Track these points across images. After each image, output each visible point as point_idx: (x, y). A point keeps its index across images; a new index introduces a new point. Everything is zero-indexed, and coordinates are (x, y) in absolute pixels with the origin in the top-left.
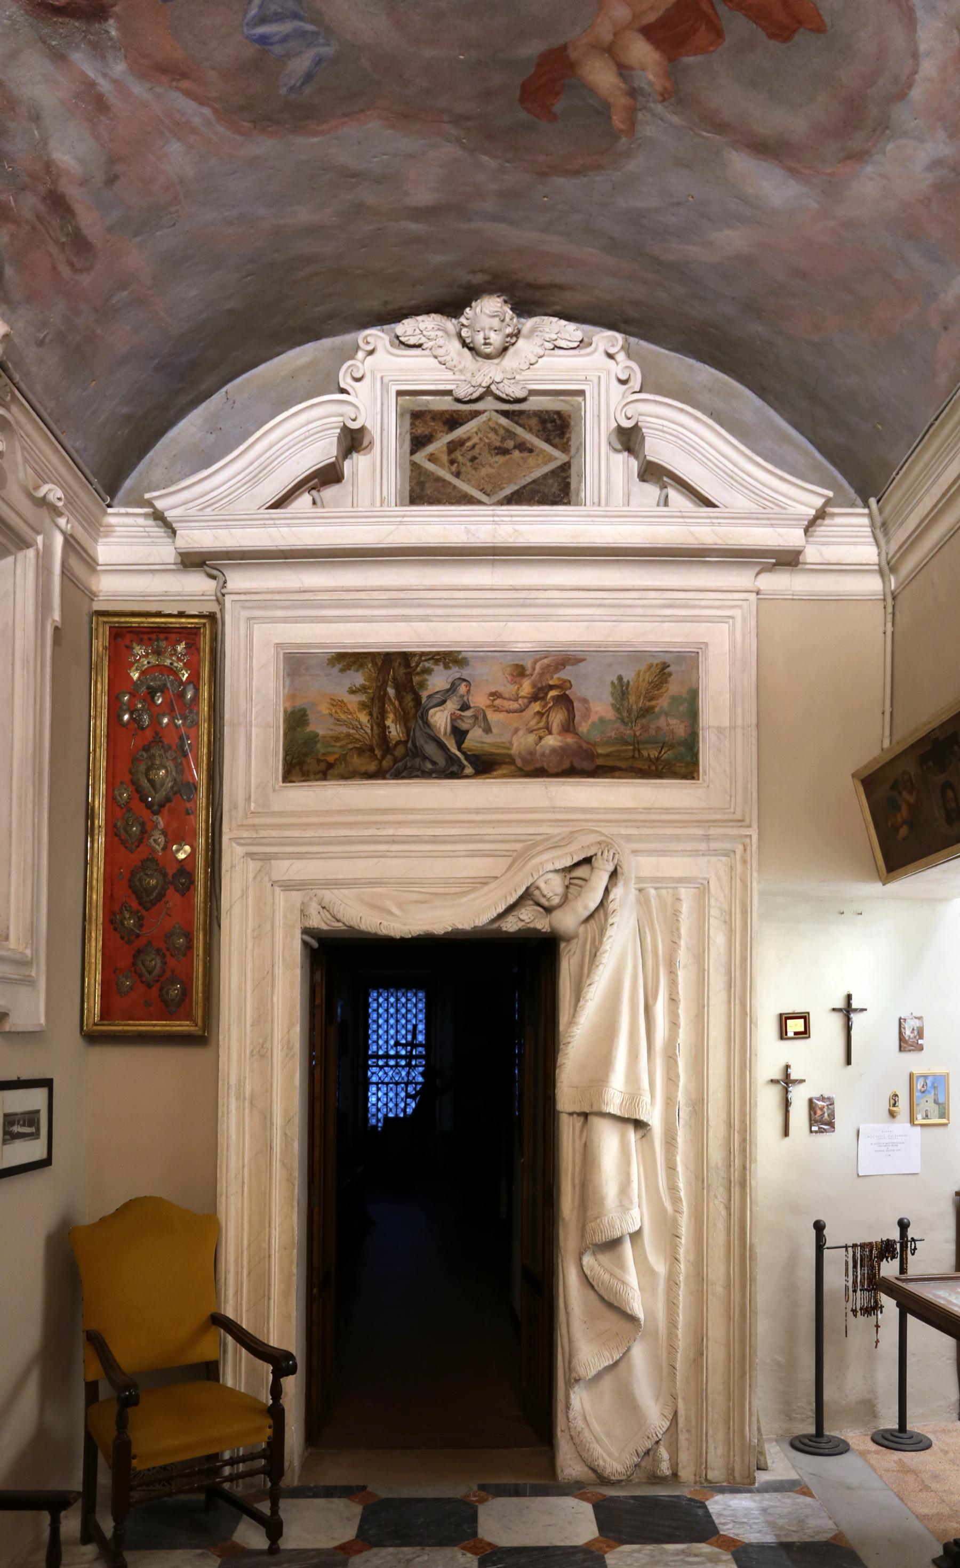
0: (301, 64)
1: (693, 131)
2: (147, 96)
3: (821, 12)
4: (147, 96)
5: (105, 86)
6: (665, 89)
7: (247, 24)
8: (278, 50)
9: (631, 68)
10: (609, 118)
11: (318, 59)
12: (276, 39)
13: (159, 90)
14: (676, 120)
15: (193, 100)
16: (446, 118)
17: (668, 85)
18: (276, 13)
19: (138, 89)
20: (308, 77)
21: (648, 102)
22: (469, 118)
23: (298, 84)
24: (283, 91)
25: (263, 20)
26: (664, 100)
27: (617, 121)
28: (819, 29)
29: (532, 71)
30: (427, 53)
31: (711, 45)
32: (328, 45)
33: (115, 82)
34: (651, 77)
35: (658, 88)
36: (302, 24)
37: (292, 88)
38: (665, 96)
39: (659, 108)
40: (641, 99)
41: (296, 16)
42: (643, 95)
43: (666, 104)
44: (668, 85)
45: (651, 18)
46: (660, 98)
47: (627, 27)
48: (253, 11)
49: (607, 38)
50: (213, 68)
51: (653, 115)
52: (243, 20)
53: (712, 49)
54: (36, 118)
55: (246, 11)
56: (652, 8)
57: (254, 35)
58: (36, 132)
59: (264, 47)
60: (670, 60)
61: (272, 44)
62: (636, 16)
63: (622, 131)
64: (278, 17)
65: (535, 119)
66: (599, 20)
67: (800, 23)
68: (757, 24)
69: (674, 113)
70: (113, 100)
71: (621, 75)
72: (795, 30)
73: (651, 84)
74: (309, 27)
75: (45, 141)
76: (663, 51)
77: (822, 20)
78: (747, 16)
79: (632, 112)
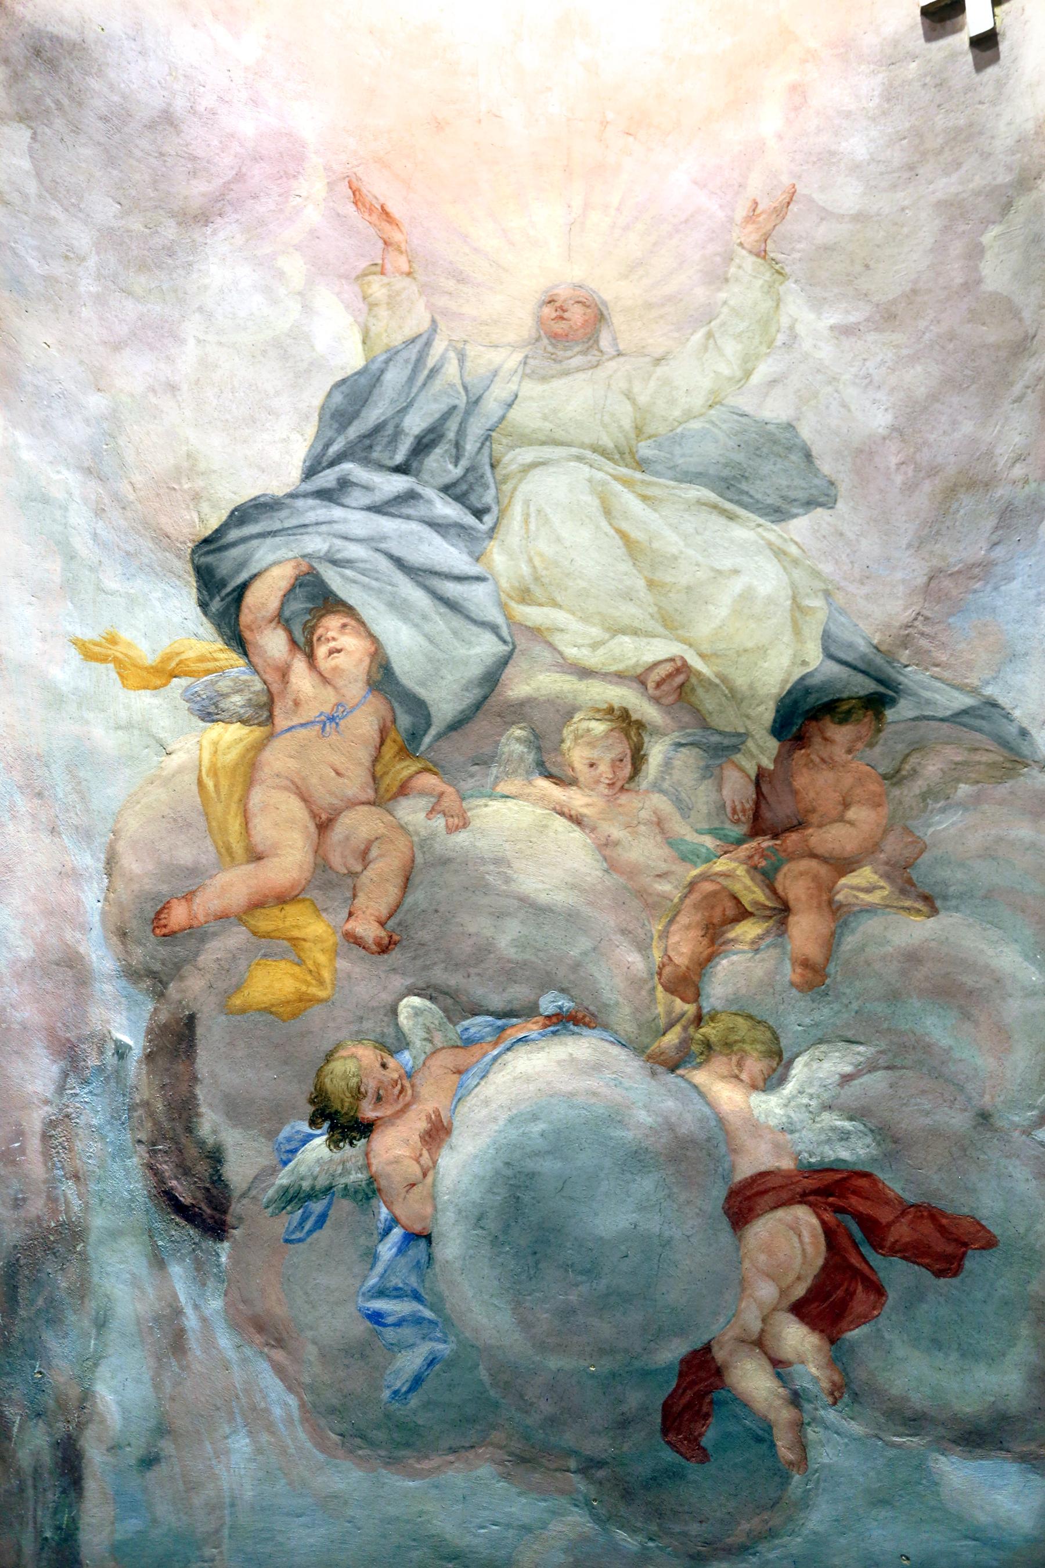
0: (410, 1362)
1: (880, 1439)
2: (231, 1354)
3: (983, 1222)
4: (231, 1354)
5: (191, 1321)
6: (834, 1384)
7: (363, 1294)
8: (390, 1334)
9: (789, 1364)
10: (773, 1445)
11: (431, 1357)
12: (390, 1320)
13: (248, 1352)
14: (856, 1428)
15: (282, 1380)
16: (573, 1464)
17: (836, 1378)
18: (396, 1289)
19: (225, 1341)
20: (417, 1381)
21: (816, 1409)
22: (601, 1464)
23: (404, 1389)
24: (386, 1394)
25: (381, 1293)
26: (835, 1403)
27: (785, 1452)
28: (990, 1243)
29: (674, 1384)
30: (554, 1363)
31: (874, 1308)
32: (445, 1342)
33: (204, 1320)
34: (814, 1370)
35: (825, 1385)
36: (421, 1308)
37: (396, 1392)
38: (836, 1394)
39: (831, 1415)
40: (807, 1406)
41: (417, 1297)
42: (809, 1401)
43: (840, 1405)
44: (836, 1378)
45: (800, 1291)
46: (830, 1400)
47: (775, 1309)
48: (373, 1281)
49: (755, 1326)
50: (315, 1343)
51: (826, 1428)
52: (360, 1288)
53: (876, 1313)
54: (101, 1324)
55: (365, 1278)
56: (799, 1278)
57: (368, 1309)
58: (93, 1342)
59: (376, 1326)
60: (832, 1341)
61: (385, 1325)
62: (783, 1292)
63: (791, 1464)
64: (397, 1293)
65: (684, 1462)
66: (743, 1305)
67: (965, 1245)
68: (918, 1264)
69: (852, 1418)
70: (193, 1343)
71: (779, 1376)
72: (964, 1254)
73: (816, 1380)
74: (428, 1314)
75: (96, 1360)
76: (822, 1331)
77: (989, 1232)
78: (904, 1258)
79: (799, 1426)
